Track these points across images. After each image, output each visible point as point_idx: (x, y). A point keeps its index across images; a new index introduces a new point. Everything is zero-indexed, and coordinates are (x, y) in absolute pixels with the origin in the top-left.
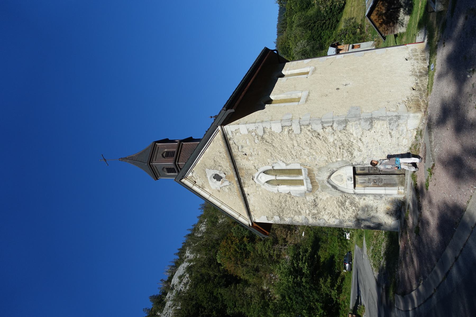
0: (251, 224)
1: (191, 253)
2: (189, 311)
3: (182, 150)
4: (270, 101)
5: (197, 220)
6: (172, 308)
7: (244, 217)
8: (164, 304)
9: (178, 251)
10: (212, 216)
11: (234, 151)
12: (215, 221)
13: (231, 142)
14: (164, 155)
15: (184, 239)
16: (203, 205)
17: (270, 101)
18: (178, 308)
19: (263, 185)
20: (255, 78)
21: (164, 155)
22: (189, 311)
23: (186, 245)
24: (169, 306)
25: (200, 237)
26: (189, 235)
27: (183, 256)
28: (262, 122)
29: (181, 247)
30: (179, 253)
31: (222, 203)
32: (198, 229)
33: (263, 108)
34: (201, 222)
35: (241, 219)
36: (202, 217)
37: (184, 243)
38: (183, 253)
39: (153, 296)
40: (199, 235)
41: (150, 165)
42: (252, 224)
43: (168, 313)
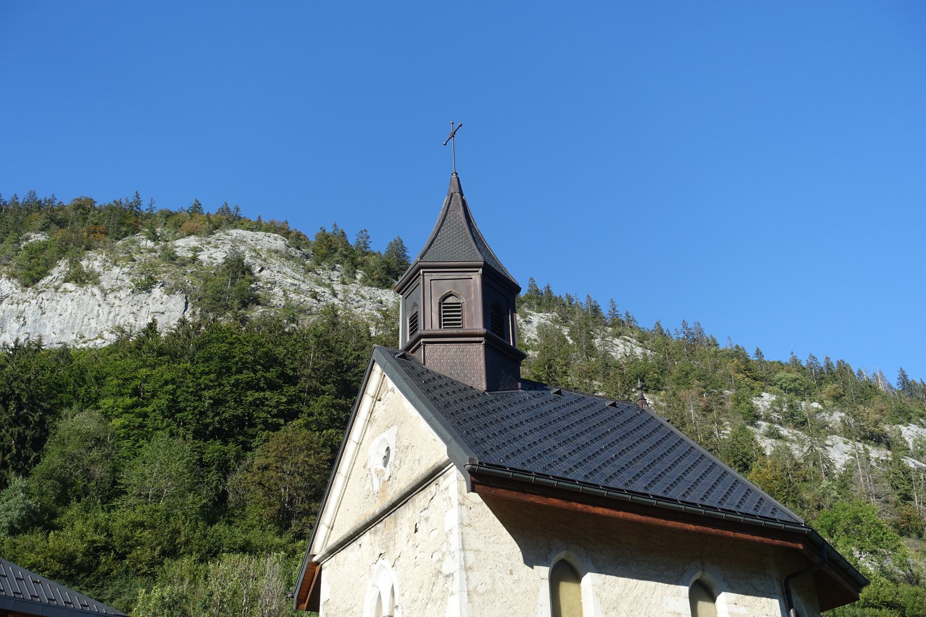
0: (315, 559)
1: (541, 329)
2: (356, 366)
3: (463, 346)
4: (564, 574)
5: (646, 323)
6: (378, 310)
7: (327, 538)
8: (384, 284)
9: (541, 287)
10: (663, 370)
11: (420, 499)
12: (648, 383)
13: (433, 488)
14: (450, 300)
15: (581, 299)
16: (701, 332)
17: (564, 574)
18: (373, 329)
19: (373, 585)
20: (640, 524)
21: (450, 300)
22: (356, 366)
23: (564, 308)
24: (381, 302)
25: (591, 347)
26: (596, 310)
27: (530, 307)
28: (467, 569)
29: (556, 293)
30: (537, 291)
31: (348, 478)
32: (618, 335)
33: (530, 561)
34: (642, 339)
35: (322, 531)
36: (653, 338)
37: (570, 300)
38: (539, 304)
39: (403, 249)
40: (597, 342)
41: (419, 269)
42: (317, 563)
43: (363, 302)
